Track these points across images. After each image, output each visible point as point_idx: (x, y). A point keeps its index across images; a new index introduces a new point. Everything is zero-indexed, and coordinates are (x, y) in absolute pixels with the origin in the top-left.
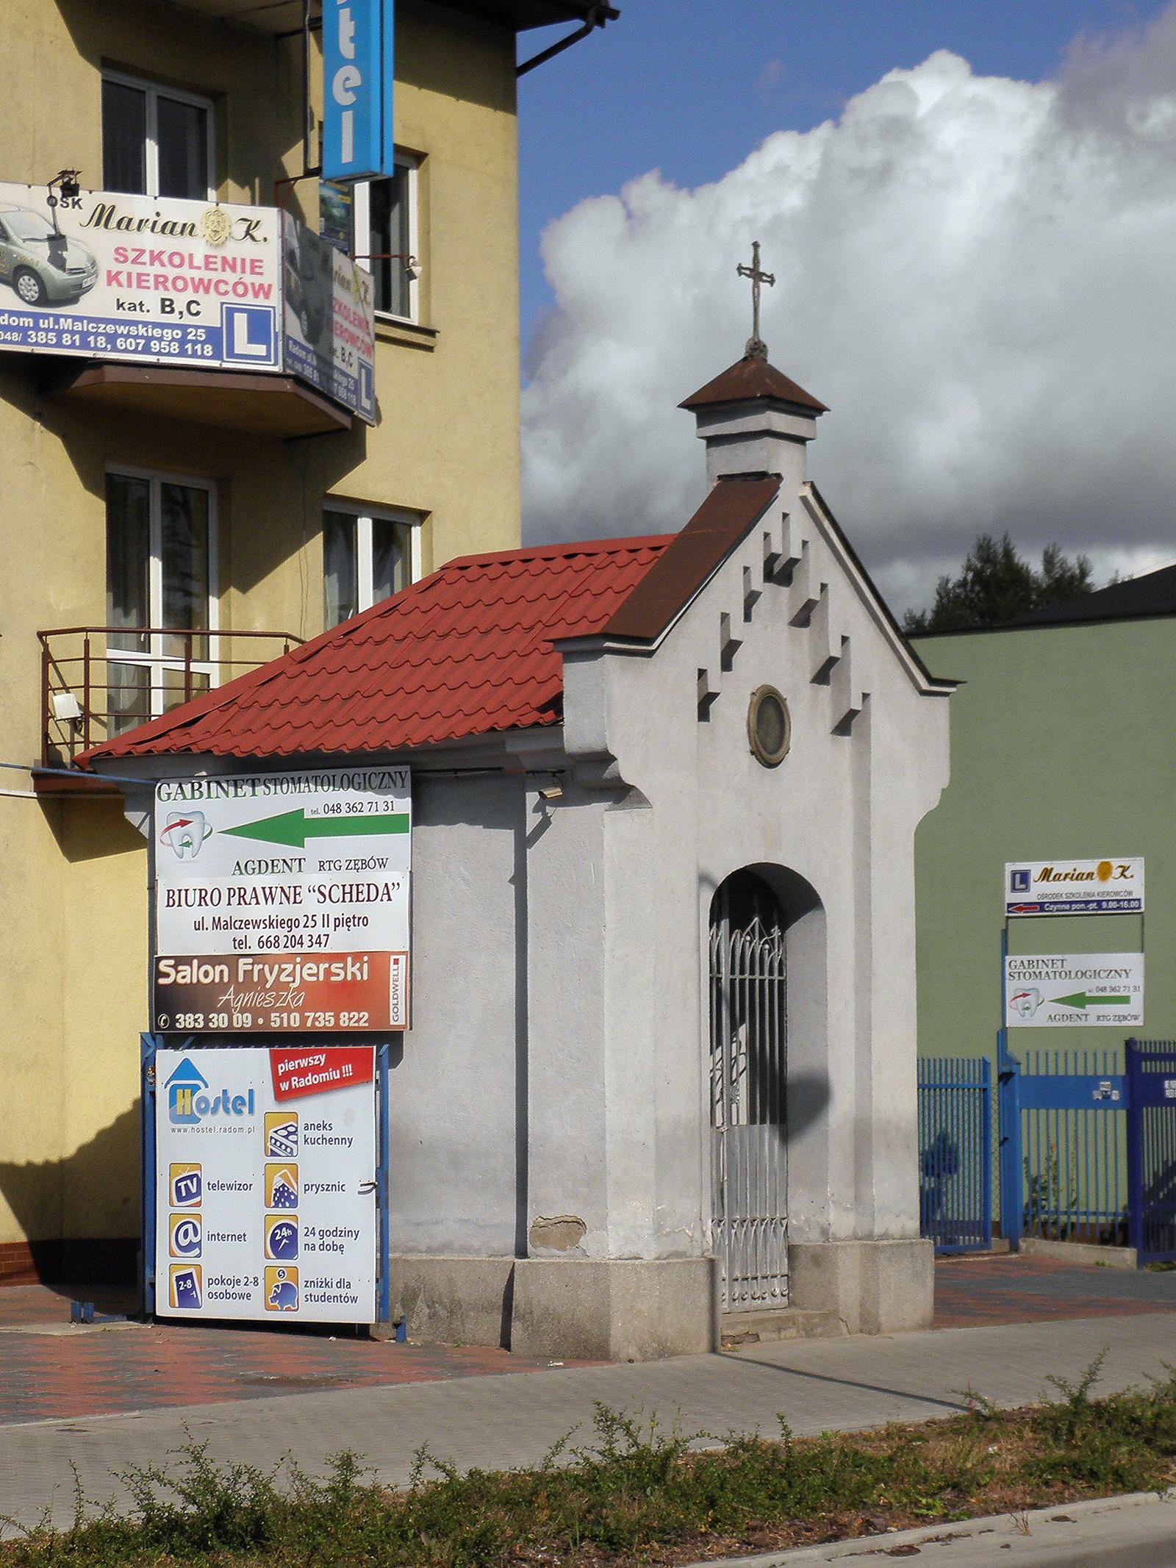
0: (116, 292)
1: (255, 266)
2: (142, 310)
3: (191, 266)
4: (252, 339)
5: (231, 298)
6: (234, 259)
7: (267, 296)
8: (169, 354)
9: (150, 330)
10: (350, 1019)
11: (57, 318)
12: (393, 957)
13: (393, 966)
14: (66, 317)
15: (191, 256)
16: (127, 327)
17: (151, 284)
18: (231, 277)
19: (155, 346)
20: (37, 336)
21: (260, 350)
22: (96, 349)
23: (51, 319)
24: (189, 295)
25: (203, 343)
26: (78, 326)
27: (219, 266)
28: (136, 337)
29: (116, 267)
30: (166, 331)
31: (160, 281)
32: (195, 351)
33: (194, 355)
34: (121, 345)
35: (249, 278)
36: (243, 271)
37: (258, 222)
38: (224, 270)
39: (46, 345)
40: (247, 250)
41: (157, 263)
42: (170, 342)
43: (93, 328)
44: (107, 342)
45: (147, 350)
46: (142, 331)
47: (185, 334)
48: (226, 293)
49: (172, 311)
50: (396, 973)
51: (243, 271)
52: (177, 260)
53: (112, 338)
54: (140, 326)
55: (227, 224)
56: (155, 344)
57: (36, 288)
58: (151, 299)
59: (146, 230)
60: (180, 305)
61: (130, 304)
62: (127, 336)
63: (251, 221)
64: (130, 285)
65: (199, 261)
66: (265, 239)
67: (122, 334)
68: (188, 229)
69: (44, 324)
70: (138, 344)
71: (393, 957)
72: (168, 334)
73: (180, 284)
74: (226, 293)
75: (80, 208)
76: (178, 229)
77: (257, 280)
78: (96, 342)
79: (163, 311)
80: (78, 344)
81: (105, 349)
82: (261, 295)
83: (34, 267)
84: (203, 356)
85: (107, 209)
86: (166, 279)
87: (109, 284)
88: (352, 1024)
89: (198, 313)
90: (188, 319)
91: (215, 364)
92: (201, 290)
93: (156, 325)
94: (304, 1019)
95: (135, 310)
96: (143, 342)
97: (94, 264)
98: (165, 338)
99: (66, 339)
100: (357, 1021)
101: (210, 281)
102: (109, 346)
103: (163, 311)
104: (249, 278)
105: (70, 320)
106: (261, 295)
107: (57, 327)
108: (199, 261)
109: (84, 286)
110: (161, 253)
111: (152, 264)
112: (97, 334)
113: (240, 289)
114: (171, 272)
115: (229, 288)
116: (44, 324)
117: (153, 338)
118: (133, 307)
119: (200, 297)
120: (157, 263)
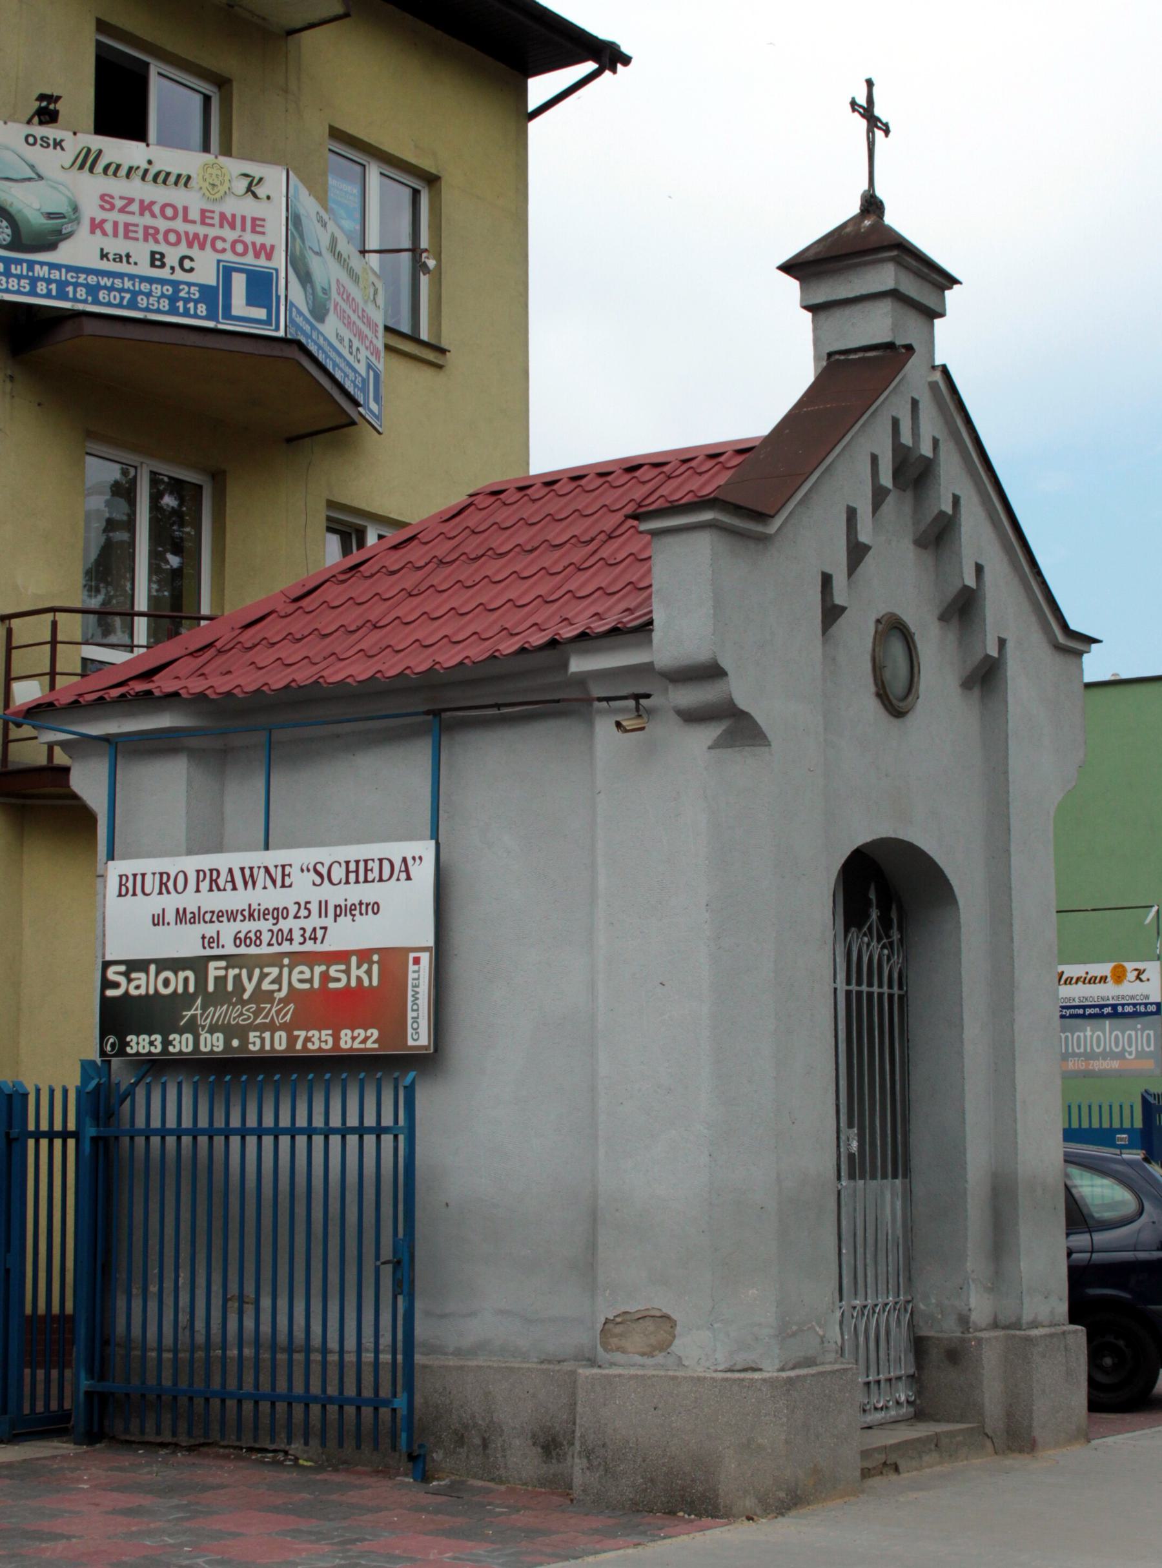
0: (99, 241)
1: (257, 225)
2: (128, 262)
3: (186, 219)
4: (251, 301)
5: (229, 256)
6: (234, 216)
7: (269, 257)
8: (158, 311)
9: (137, 284)
10: (354, 1039)
11: (31, 265)
12: (412, 955)
13: (412, 967)
14: (42, 264)
15: (185, 209)
16: (111, 280)
17: (140, 235)
18: (230, 235)
19: (142, 301)
20: (7, 282)
21: (260, 313)
22: (75, 300)
23: (25, 265)
24: (183, 249)
25: (196, 302)
26: (55, 275)
27: (216, 221)
28: (120, 291)
29: (100, 215)
30: (154, 286)
31: (150, 233)
32: (187, 310)
33: (186, 314)
34: (104, 298)
35: (249, 237)
36: (243, 229)
37: (261, 179)
38: (221, 226)
39: (18, 292)
40: (248, 208)
41: (147, 213)
42: (159, 298)
43: (72, 277)
44: (88, 294)
45: (133, 305)
46: (128, 284)
47: (177, 291)
48: (224, 250)
49: (163, 265)
50: (416, 976)
51: (243, 229)
52: (169, 212)
53: (93, 290)
54: (126, 279)
55: (227, 178)
56: (142, 299)
57: (9, 231)
58: (141, 251)
59: (136, 178)
60: (172, 259)
61: (115, 255)
62: (111, 289)
63: (254, 178)
64: (116, 235)
65: (194, 215)
66: (268, 198)
67: (105, 287)
68: (183, 181)
69: (16, 269)
70: (122, 298)
71: (412, 955)
72: (157, 289)
73: (172, 238)
74: (224, 250)
75: (62, 149)
76: (172, 179)
77: (259, 240)
78: (75, 292)
79: (153, 265)
80: (54, 293)
81: (85, 301)
82: (263, 255)
83: (8, 208)
84: (196, 316)
85: (92, 152)
86: (157, 231)
87: (93, 232)
88: (356, 1045)
89: (191, 270)
90: (179, 275)
91: (210, 324)
92: (196, 245)
93: (143, 279)
94: (292, 1040)
95: (121, 261)
96: (128, 296)
97: (76, 209)
98: (154, 294)
99: (41, 287)
100: (364, 1041)
101: (206, 236)
102: (90, 299)
103: (153, 265)
104: (249, 237)
105: (46, 268)
106: (263, 255)
107: (30, 274)
108: (194, 215)
109: (64, 231)
110: (152, 203)
111: (142, 214)
112: (76, 285)
113: (240, 248)
114: (162, 225)
115: (228, 246)
116: (16, 269)
117: (141, 292)
118: (119, 258)
119: (195, 252)
120: (147, 213)
